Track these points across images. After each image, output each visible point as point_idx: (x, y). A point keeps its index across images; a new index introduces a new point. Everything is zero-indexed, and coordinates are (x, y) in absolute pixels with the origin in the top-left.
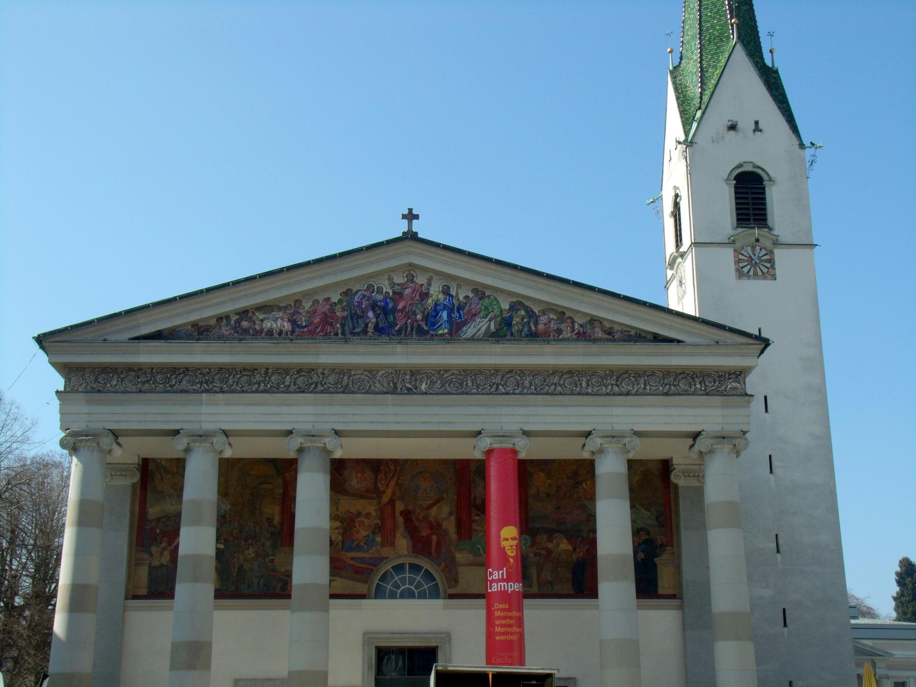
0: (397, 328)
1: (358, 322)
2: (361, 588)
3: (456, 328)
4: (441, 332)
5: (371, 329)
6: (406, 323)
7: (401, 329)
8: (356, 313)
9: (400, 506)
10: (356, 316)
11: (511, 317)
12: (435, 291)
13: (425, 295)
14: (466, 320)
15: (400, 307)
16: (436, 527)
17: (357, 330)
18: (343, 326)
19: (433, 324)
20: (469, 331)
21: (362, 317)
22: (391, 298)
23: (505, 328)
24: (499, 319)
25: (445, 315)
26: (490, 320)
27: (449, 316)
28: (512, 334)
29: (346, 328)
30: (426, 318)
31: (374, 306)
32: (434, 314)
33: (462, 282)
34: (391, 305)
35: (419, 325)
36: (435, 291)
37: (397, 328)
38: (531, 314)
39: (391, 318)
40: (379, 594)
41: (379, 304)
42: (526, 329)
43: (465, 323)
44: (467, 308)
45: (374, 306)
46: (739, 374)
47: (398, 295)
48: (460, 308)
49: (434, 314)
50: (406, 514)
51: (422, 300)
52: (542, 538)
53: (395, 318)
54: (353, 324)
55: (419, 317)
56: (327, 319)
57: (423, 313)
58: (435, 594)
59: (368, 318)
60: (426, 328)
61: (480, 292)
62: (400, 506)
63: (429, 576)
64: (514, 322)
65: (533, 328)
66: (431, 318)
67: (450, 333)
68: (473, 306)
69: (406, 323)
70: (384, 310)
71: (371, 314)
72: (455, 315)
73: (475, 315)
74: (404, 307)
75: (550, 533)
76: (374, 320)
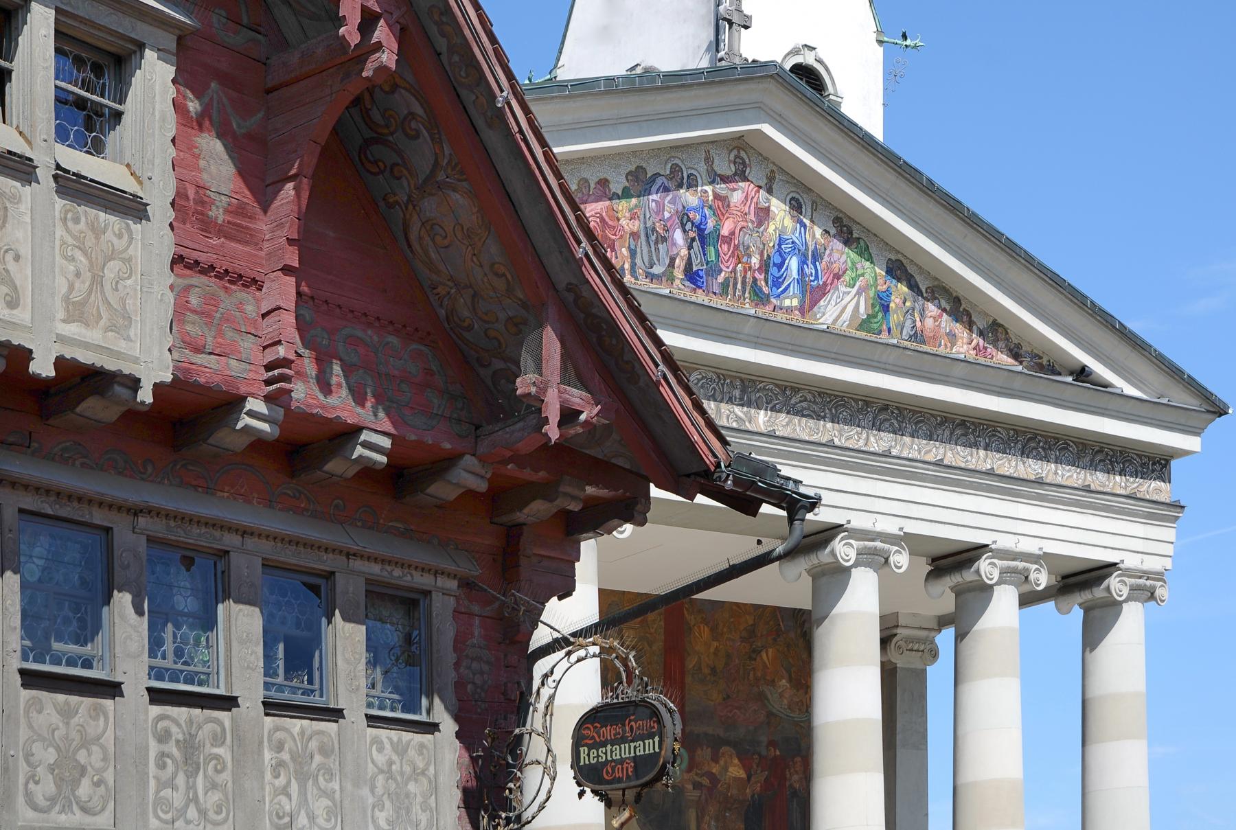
0: (721, 279)
1: (657, 250)
3: (813, 295)
4: (787, 303)
5: (679, 273)
6: (734, 270)
7: (727, 279)
8: (654, 230)
11: (888, 293)
14: (825, 284)
15: (725, 232)
17: (658, 270)
18: (633, 254)
19: (777, 283)
21: (664, 239)
22: (710, 207)
23: (880, 315)
24: (872, 293)
25: (794, 263)
26: (858, 294)
27: (801, 271)
28: (889, 330)
29: (638, 261)
30: (765, 266)
32: (778, 260)
34: (711, 223)
35: (755, 280)
37: (721, 279)
39: (712, 256)
41: (691, 215)
42: (908, 324)
43: (822, 291)
44: (826, 259)
48: (817, 257)
49: (778, 260)
51: (760, 224)
53: (718, 255)
54: (650, 252)
55: (755, 261)
57: (762, 254)
59: (674, 244)
60: (766, 290)
64: (892, 305)
65: (918, 324)
66: (772, 266)
67: (802, 310)
68: (836, 256)
69: (734, 270)
71: (678, 236)
72: (809, 270)
73: (838, 277)
74: (733, 233)
76: (684, 252)
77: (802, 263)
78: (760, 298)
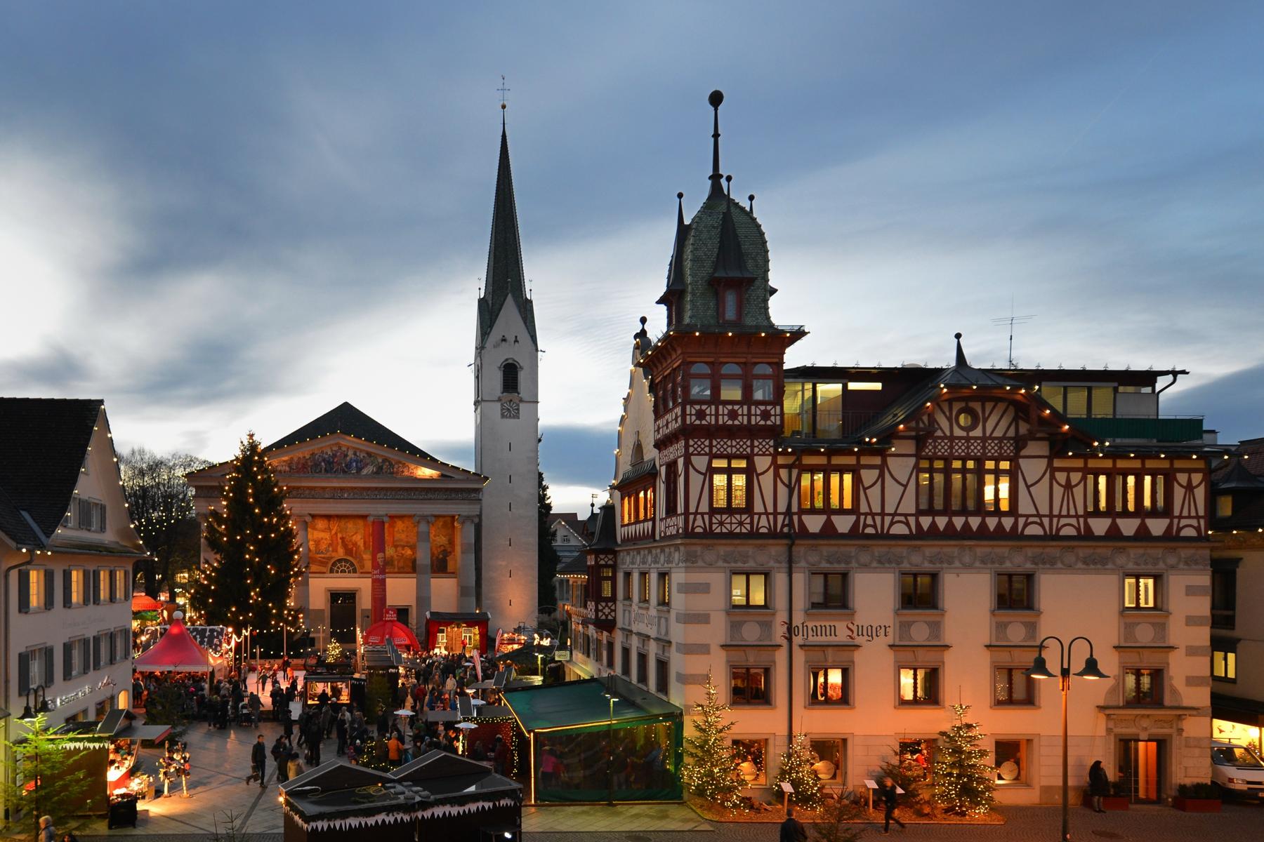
2: (324, 569)
3: (359, 470)
9: (339, 535)
10: (317, 465)
12: (350, 453)
13: (346, 456)
16: (355, 544)
20: (365, 472)
31: (324, 460)
33: (361, 451)
36: (350, 453)
38: (391, 464)
40: (332, 571)
45: (324, 460)
46: (478, 491)
47: (334, 456)
50: (342, 538)
52: (399, 549)
56: (304, 466)
58: (355, 571)
61: (369, 454)
62: (339, 535)
63: (352, 564)
66: (349, 466)
70: (328, 463)
75: (403, 547)
77: (357, 462)
78: (345, 472)
